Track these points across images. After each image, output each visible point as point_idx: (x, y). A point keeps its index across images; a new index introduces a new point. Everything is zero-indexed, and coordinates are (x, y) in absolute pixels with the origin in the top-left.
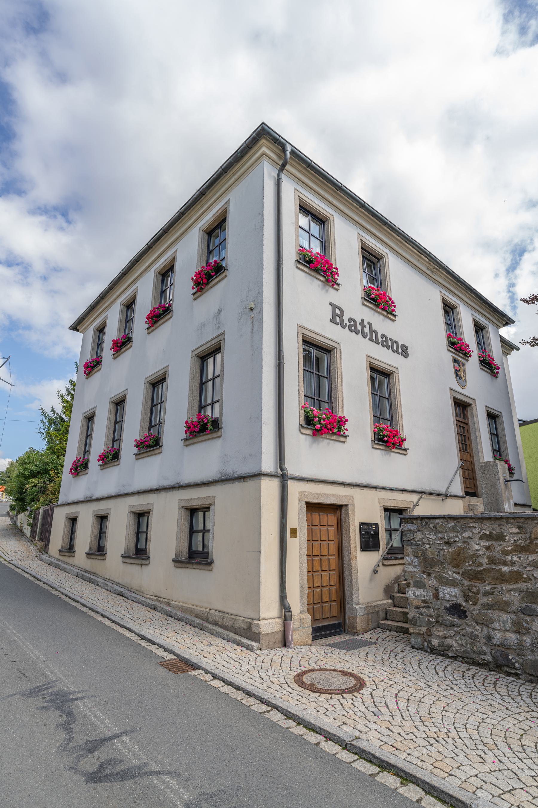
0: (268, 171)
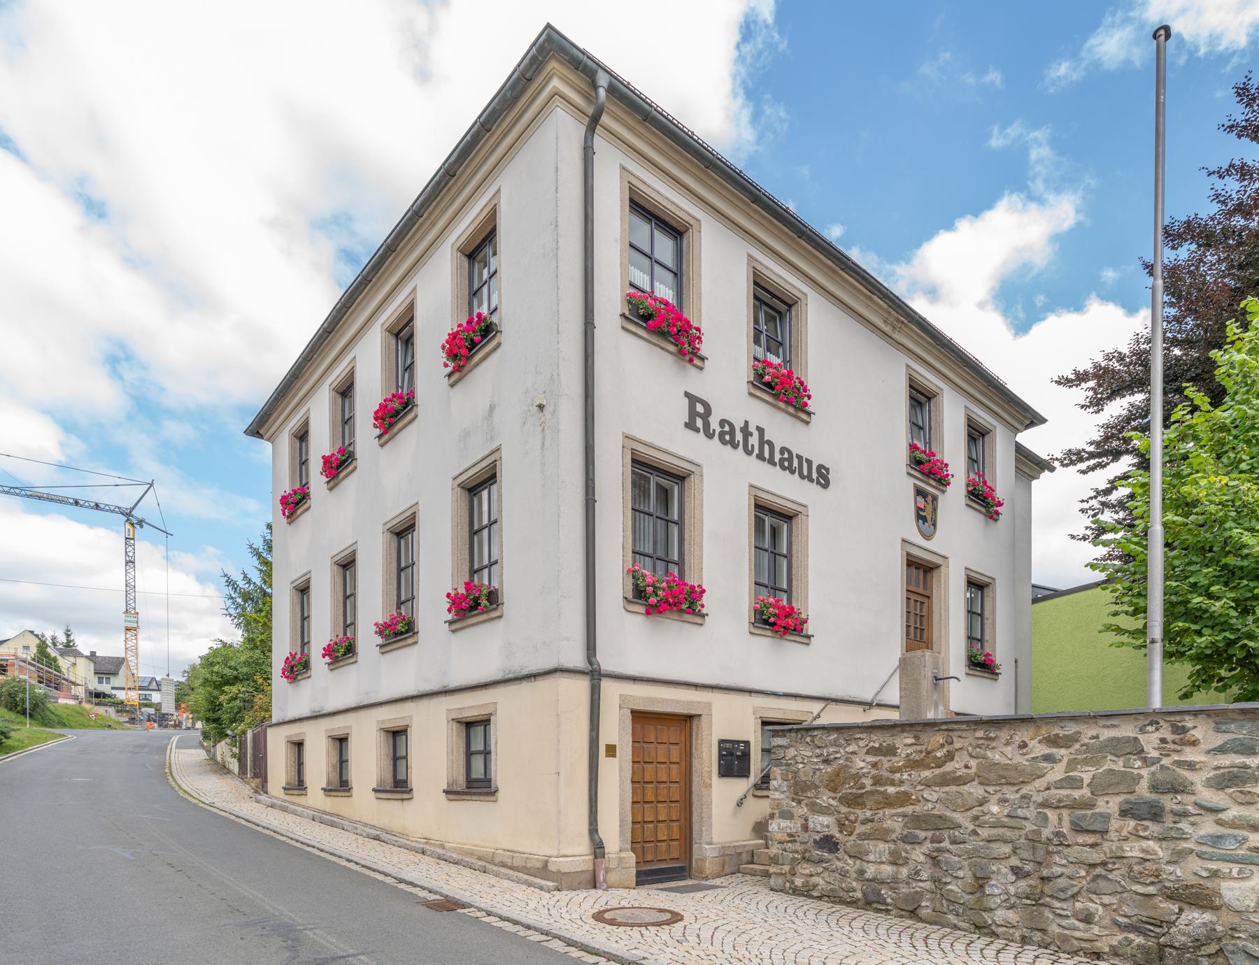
0: (560, 131)
